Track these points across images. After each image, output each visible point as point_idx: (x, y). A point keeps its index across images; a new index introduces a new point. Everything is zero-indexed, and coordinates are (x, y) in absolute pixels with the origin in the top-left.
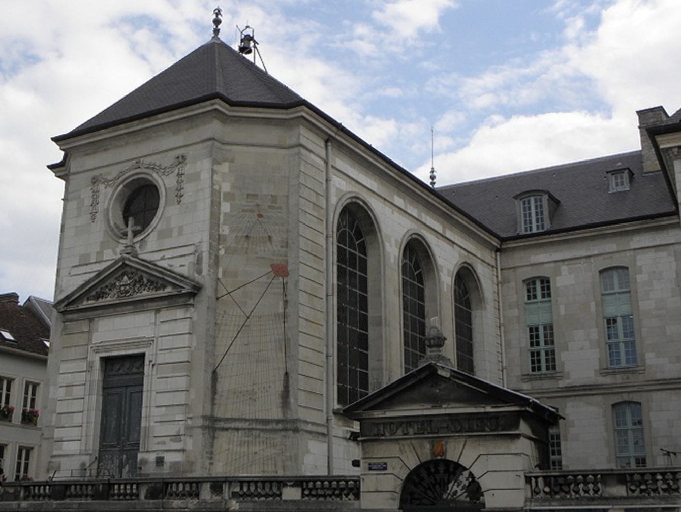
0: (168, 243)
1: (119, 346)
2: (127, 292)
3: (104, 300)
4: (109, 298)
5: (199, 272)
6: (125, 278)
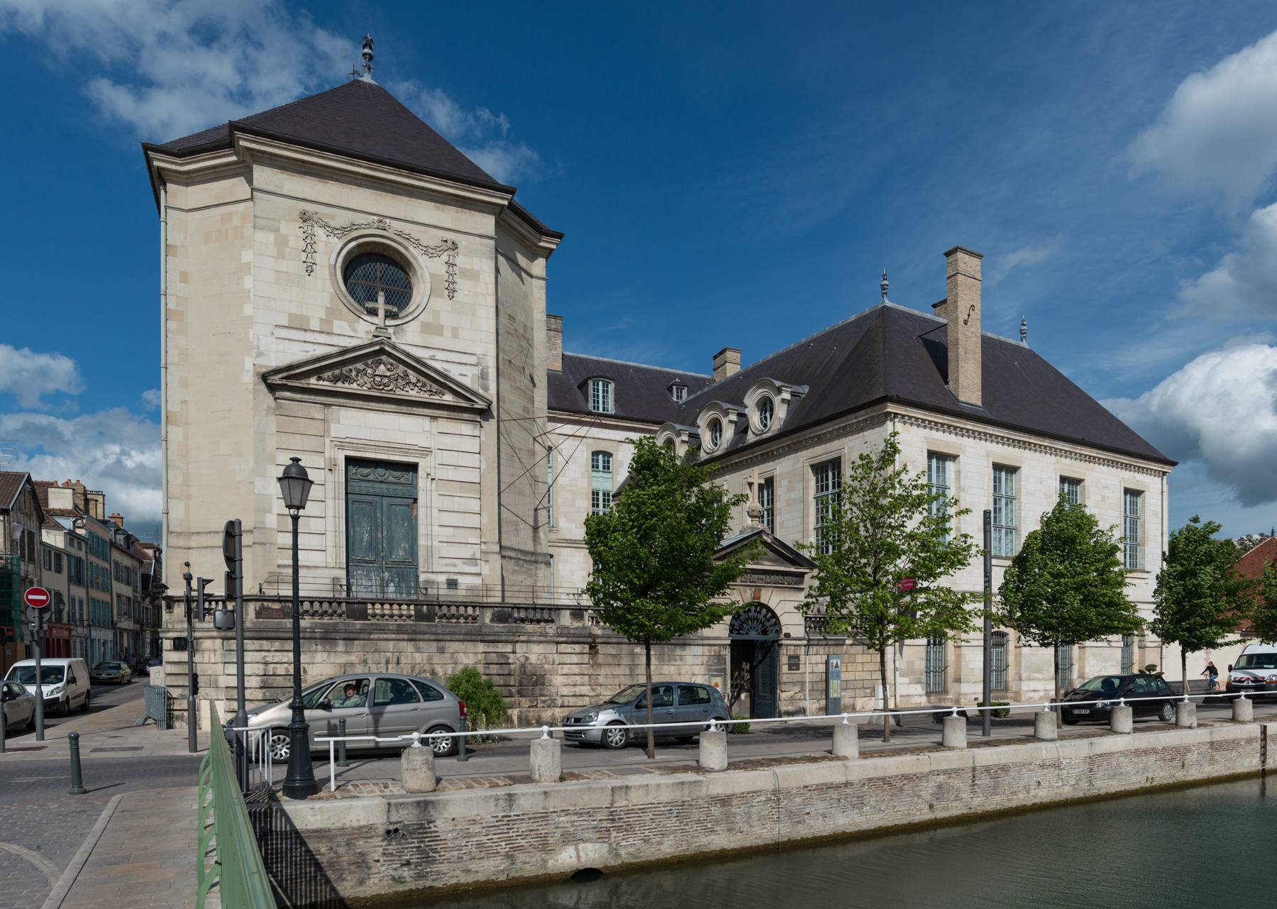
0: (435, 341)
1: (377, 447)
2: (385, 385)
3: (346, 385)
4: (355, 385)
5: (486, 389)
6: (382, 367)
